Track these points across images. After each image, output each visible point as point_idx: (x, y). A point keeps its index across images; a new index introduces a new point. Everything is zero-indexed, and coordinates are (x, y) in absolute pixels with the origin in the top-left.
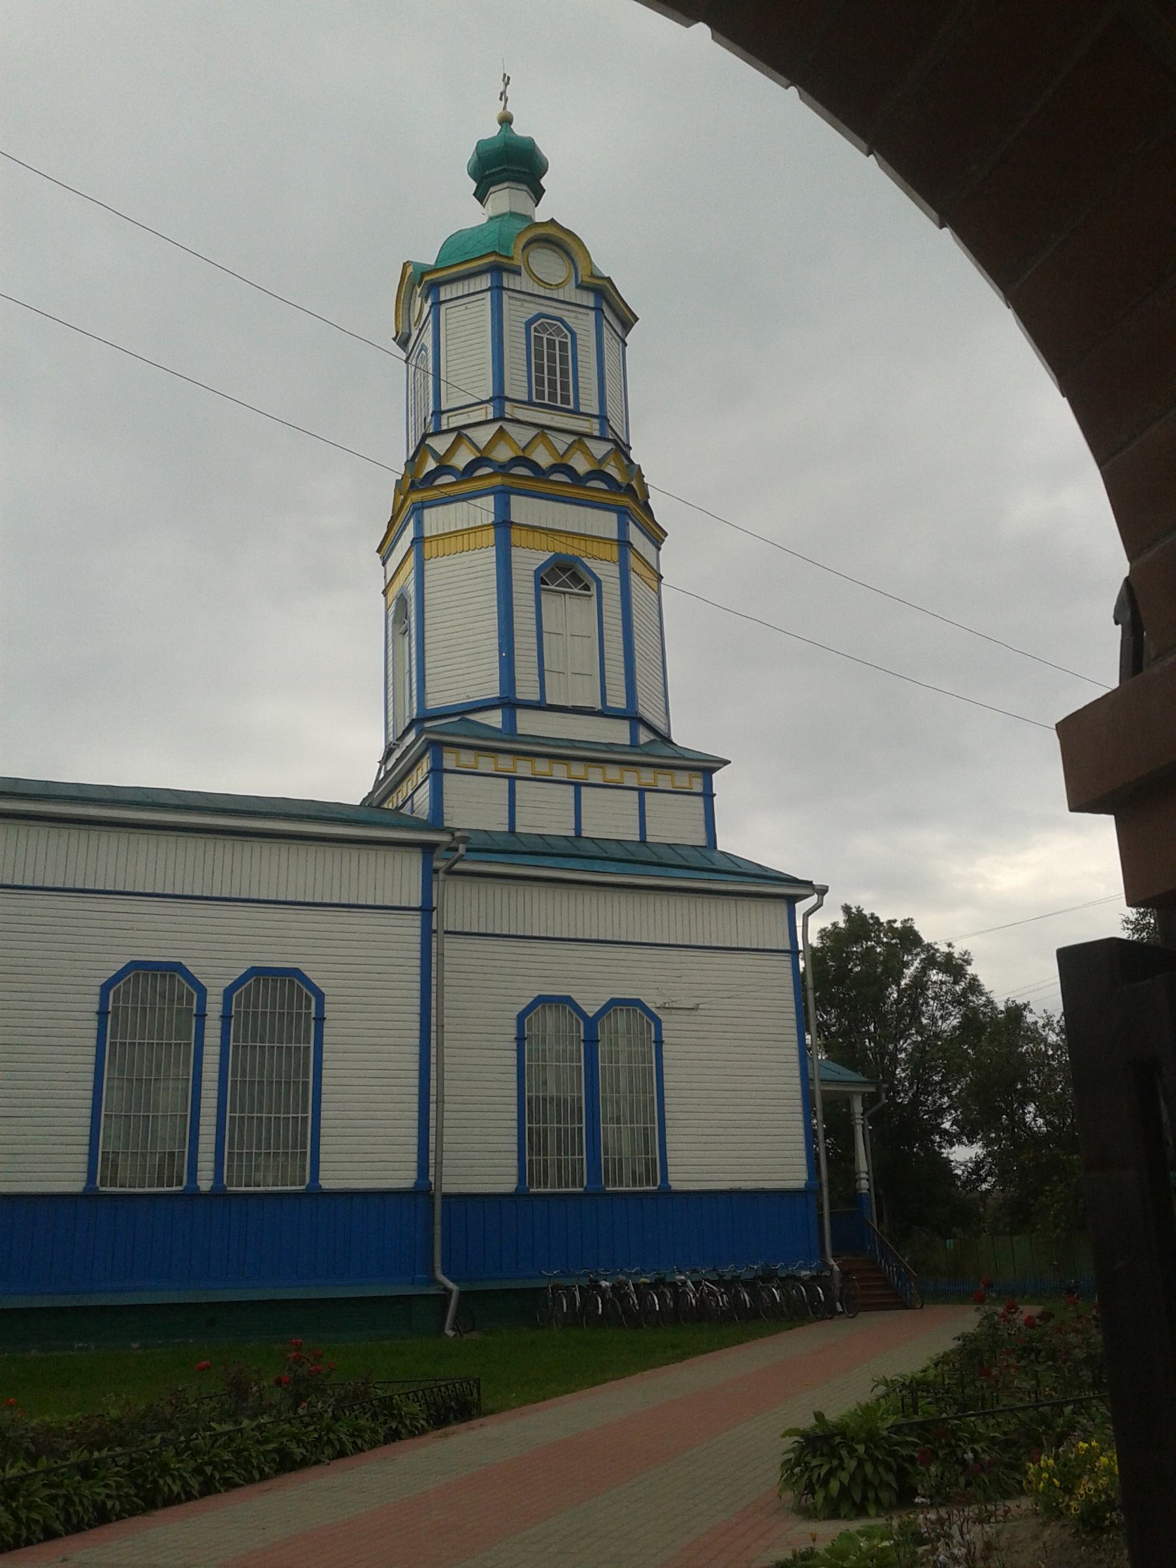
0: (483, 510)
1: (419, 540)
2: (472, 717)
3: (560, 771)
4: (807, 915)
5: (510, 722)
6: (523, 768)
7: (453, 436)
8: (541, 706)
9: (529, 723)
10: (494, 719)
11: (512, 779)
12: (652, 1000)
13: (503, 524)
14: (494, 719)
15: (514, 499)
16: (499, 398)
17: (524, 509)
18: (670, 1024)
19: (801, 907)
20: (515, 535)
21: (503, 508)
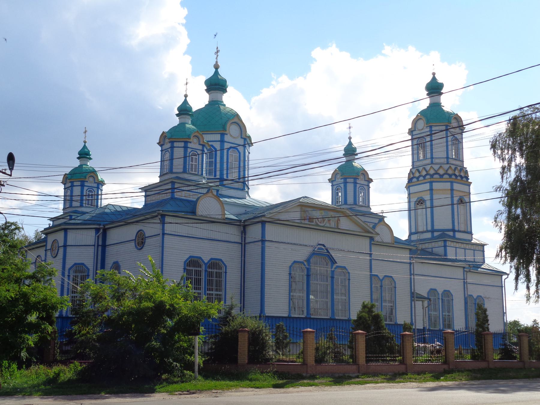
0: (448, 185)
1: (431, 190)
2: (445, 232)
3: (462, 246)
4: (505, 279)
5: (454, 235)
6: (458, 245)
7: (439, 166)
8: (459, 231)
9: (458, 235)
10: (451, 234)
11: (456, 248)
12: (483, 296)
13: (452, 190)
14: (451, 234)
15: (455, 185)
16: (447, 158)
17: (456, 186)
18: (486, 300)
19: (504, 277)
20: (455, 192)
21: (452, 186)
